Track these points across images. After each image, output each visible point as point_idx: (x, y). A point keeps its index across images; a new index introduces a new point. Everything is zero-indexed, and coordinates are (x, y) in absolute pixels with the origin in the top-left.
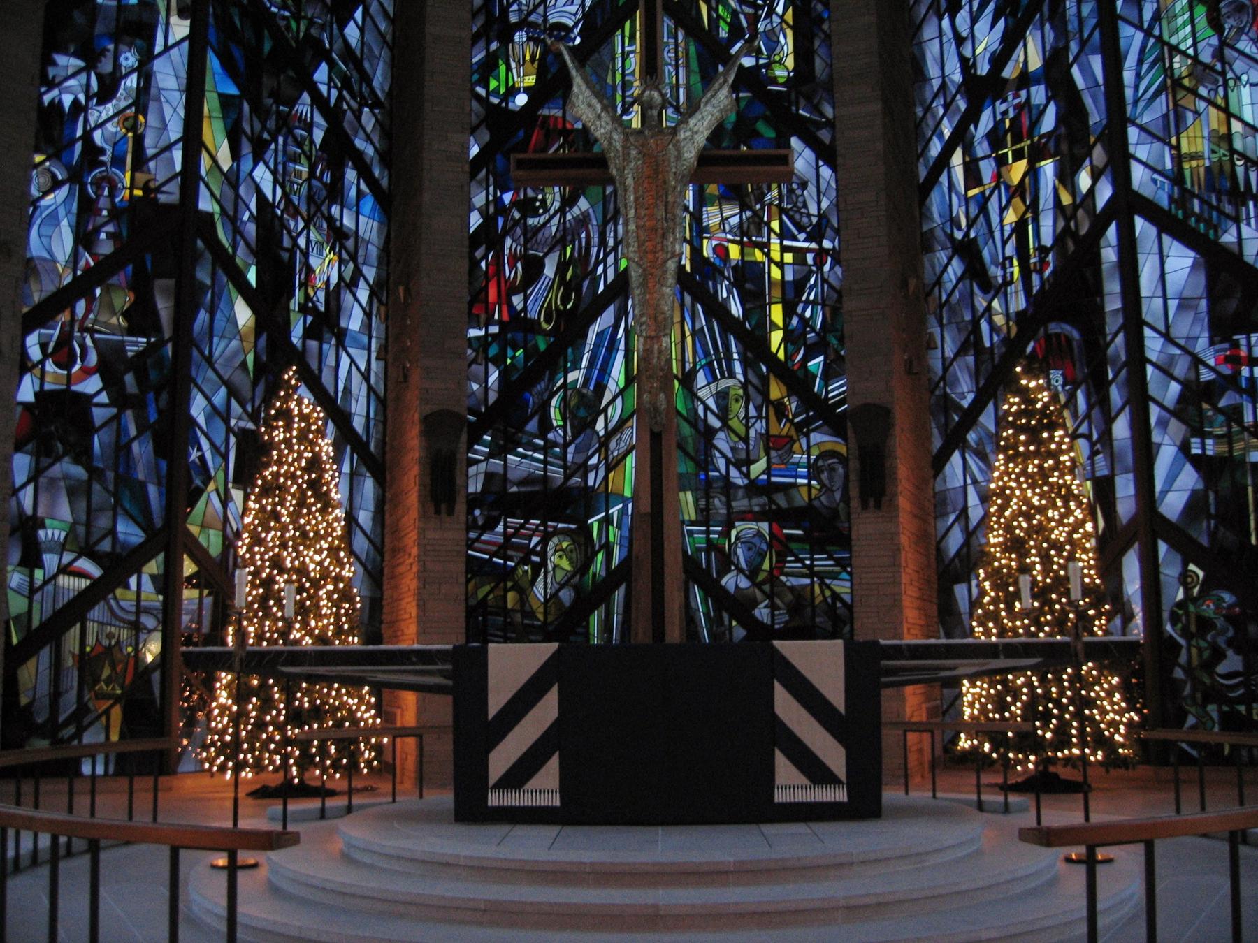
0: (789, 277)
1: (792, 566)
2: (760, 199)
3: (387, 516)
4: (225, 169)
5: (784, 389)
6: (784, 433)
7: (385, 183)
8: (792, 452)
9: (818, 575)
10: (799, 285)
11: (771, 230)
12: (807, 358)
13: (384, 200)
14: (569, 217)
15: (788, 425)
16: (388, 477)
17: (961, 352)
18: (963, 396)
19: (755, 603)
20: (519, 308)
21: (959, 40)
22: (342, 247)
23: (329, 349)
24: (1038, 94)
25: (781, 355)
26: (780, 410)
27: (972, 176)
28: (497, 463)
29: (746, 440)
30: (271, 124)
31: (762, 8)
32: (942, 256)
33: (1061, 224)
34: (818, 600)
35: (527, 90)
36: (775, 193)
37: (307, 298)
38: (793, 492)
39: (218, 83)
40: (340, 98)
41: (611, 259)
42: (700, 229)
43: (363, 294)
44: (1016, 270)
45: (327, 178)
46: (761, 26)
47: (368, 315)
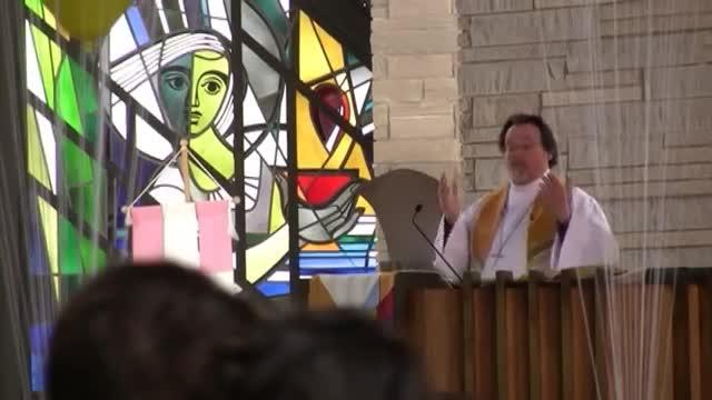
5: (335, 50)
6: (335, 163)
15: (347, 141)
29: (235, 186)
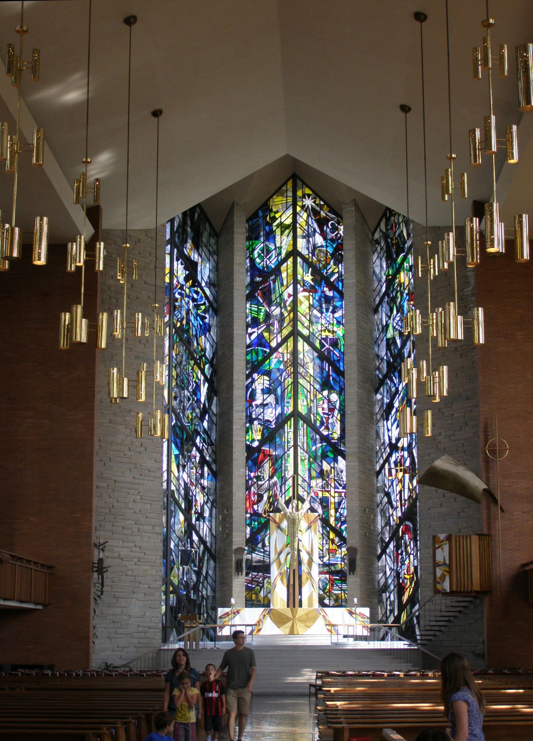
0: (337, 501)
1: (335, 587)
2: (328, 477)
3: (217, 572)
4: (176, 476)
5: (334, 535)
7: (214, 469)
8: (336, 554)
9: (343, 590)
10: (339, 503)
11: (331, 486)
12: (341, 526)
13: (214, 474)
14: (271, 482)
16: (217, 560)
17: (386, 525)
18: (386, 538)
19: (324, 599)
20: (256, 509)
21: (388, 430)
22: (204, 492)
23: (201, 523)
24: (406, 454)
25: (334, 525)
26: (333, 541)
27: (390, 474)
28: (249, 556)
29: (322, 551)
30: (186, 460)
31: (330, 415)
32: (382, 495)
33: (409, 494)
34: (343, 597)
35: (258, 440)
36: (333, 475)
37: (196, 509)
38: (336, 565)
39: (175, 451)
40: (203, 445)
41: (283, 496)
42: (310, 487)
43: (209, 505)
44: (399, 504)
45: (200, 472)
46: (330, 421)
47: (211, 511)
